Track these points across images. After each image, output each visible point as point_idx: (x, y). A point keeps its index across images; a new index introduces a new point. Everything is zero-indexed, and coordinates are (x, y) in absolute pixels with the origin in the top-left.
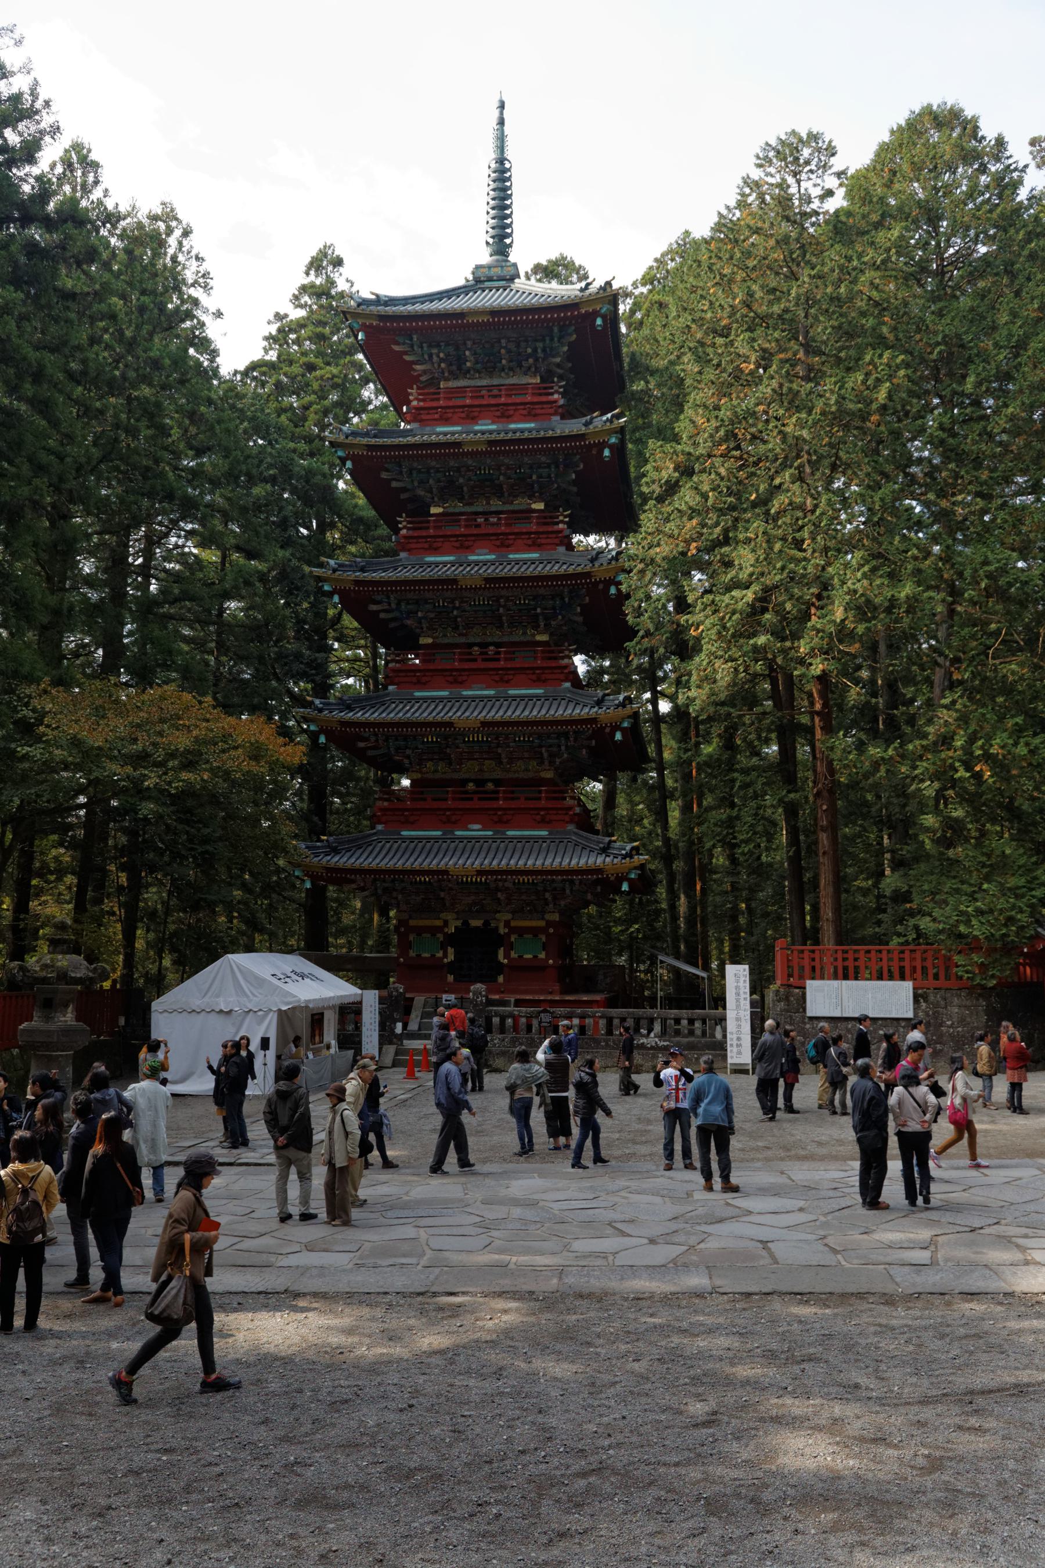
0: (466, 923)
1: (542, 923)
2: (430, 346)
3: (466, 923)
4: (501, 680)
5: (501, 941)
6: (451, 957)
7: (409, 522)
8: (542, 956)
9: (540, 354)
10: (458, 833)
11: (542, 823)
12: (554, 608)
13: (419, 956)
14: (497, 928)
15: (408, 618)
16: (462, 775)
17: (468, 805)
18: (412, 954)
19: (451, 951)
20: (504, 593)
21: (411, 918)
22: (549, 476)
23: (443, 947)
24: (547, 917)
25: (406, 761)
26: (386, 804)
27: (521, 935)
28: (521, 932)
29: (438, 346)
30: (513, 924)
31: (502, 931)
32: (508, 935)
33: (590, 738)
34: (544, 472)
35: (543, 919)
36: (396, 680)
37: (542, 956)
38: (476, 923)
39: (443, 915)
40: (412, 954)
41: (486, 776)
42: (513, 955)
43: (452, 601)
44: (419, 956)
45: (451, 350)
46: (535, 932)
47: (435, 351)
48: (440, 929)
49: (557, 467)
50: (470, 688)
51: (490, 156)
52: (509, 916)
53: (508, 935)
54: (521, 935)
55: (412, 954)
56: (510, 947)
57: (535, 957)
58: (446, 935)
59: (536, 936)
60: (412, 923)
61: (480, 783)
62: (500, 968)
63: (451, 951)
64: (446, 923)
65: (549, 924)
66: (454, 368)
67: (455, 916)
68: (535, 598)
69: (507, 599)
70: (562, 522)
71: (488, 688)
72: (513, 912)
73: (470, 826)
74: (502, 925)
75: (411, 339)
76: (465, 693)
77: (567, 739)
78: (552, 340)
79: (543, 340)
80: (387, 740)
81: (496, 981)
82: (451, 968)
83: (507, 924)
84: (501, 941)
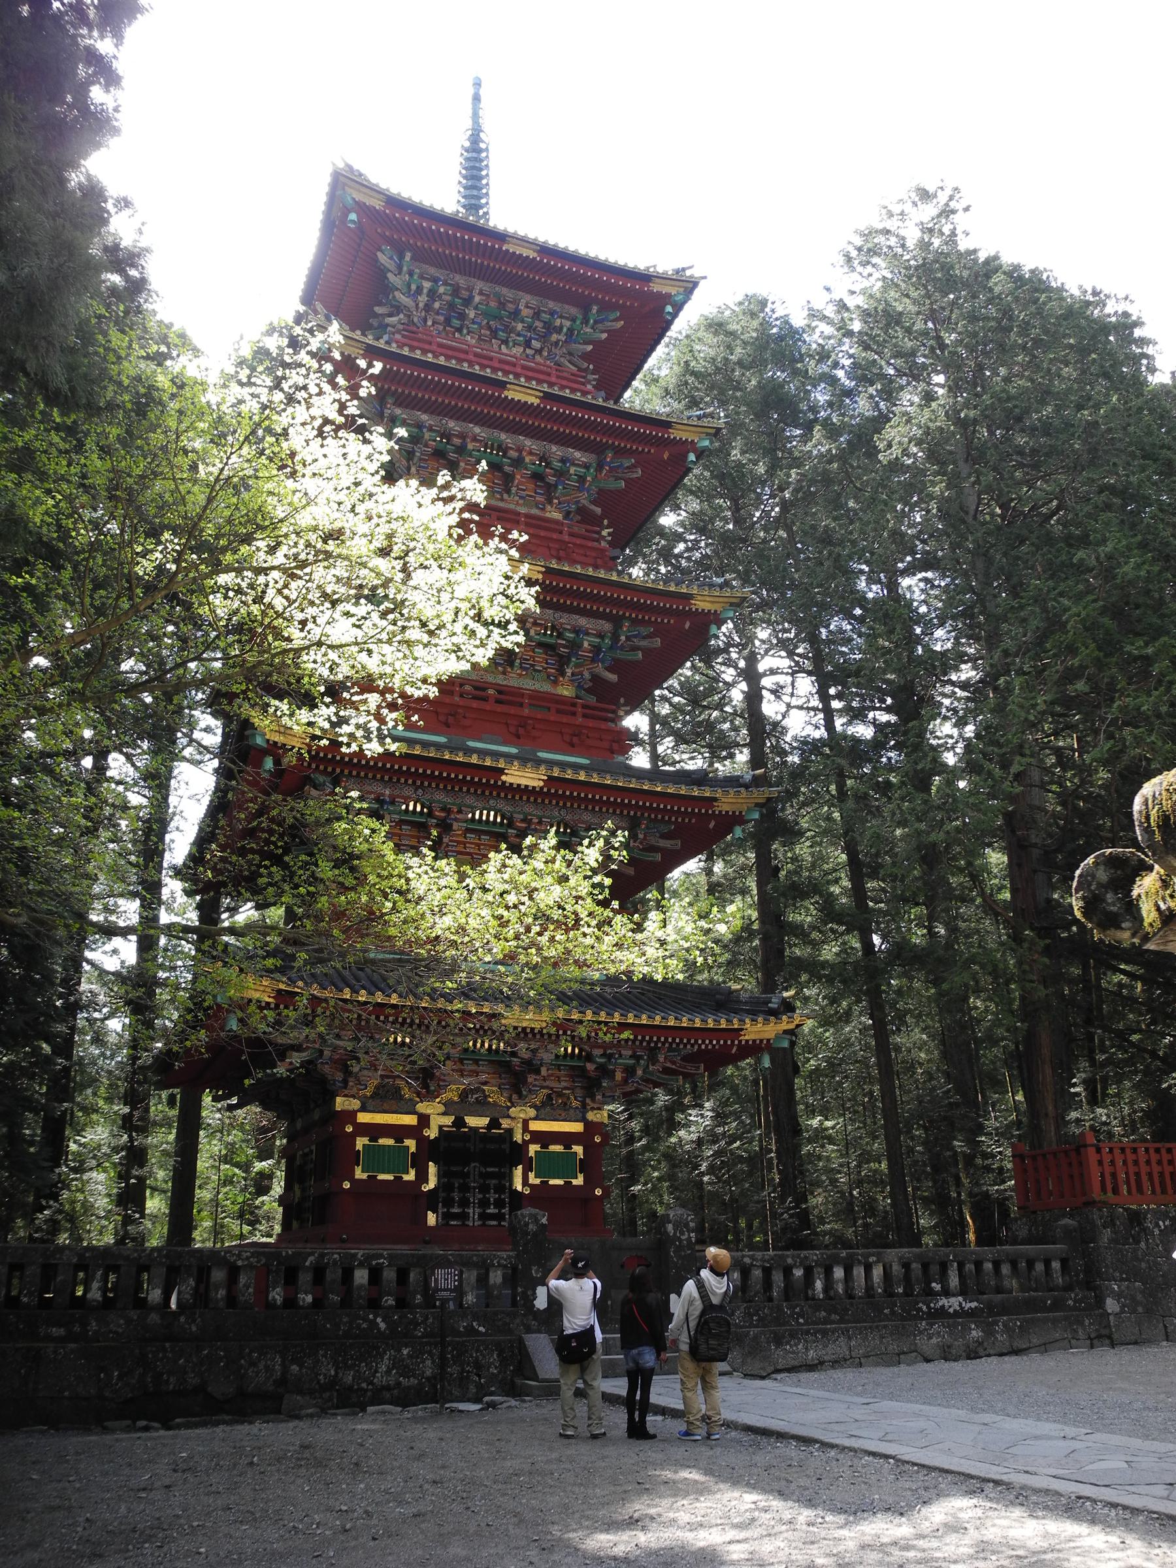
0: (459, 1122)
1: (577, 1127)
2: (422, 277)
3: (459, 1122)
6: (432, 1184)
14: (510, 1132)
18: (360, 1174)
19: (432, 1168)
21: (363, 1109)
22: (582, 479)
29: (435, 280)
30: (535, 1126)
31: (518, 1137)
32: (526, 1143)
37: (579, 1181)
38: (477, 1122)
39: (422, 1107)
40: (360, 1174)
42: (533, 1180)
46: (567, 1139)
47: (427, 285)
48: (414, 1132)
50: (480, 740)
51: (469, 123)
52: (532, 1112)
53: (526, 1143)
57: (568, 1183)
58: (422, 1141)
60: (364, 1118)
63: (432, 1168)
64: (424, 1120)
66: (441, 318)
67: (442, 1108)
68: (577, 631)
71: (505, 743)
75: (401, 257)
76: (471, 744)
78: (585, 321)
79: (573, 320)
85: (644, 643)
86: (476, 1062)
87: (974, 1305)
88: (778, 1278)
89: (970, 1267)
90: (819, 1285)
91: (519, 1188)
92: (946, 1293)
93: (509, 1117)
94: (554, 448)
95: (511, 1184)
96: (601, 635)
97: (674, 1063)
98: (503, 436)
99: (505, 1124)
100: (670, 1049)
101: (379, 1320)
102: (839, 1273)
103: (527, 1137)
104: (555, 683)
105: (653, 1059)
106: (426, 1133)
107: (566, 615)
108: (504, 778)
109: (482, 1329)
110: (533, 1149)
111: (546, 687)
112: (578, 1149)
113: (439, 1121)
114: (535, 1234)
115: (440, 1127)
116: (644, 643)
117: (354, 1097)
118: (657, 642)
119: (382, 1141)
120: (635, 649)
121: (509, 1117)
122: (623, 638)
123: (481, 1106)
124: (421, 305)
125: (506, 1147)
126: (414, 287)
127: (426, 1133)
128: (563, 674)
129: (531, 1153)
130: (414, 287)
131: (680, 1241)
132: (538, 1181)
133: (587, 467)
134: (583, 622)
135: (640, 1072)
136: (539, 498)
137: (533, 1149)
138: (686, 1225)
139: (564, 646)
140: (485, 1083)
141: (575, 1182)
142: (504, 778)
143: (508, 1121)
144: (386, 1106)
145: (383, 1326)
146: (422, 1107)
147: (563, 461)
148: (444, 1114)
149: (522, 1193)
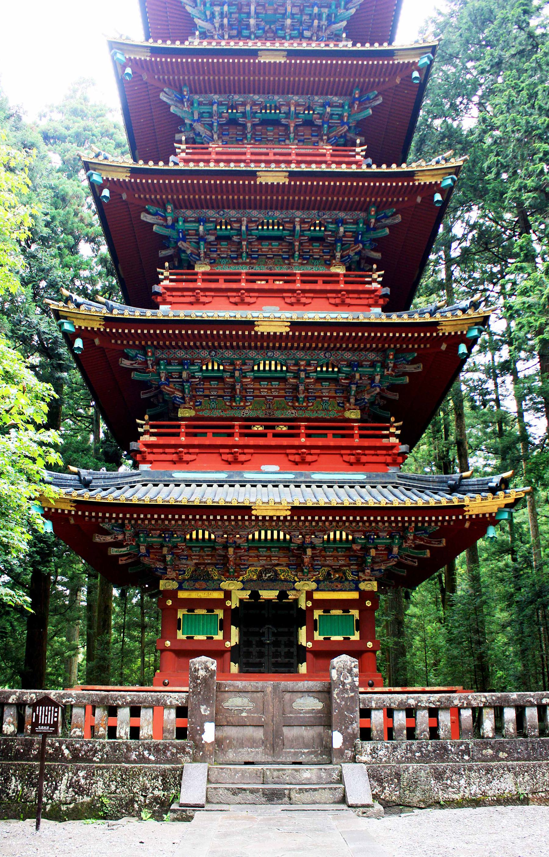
0: (255, 595)
1: (355, 595)
3: (255, 595)
4: (298, 302)
5: (302, 617)
7: (187, 148)
8: (356, 637)
9: (324, 22)
11: (356, 464)
12: (355, 234)
14: (296, 601)
15: (184, 240)
16: (248, 413)
17: (261, 441)
20: (298, 213)
21: (180, 588)
23: (223, 626)
25: (178, 394)
26: (154, 439)
28: (327, 605)
30: (317, 596)
31: (303, 604)
32: (310, 610)
33: (413, 362)
34: (338, 110)
35: (357, 589)
36: (169, 299)
37: (356, 637)
38: (269, 595)
39: (225, 585)
41: (279, 414)
42: (318, 637)
43: (239, 221)
45: (234, 9)
46: (345, 605)
47: (217, 9)
48: (219, 603)
49: (351, 106)
52: (314, 586)
53: (310, 610)
55: (181, 635)
56: (313, 626)
58: (227, 610)
59: (346, 611)
60: (182, 595)
61: (270, 422)
62: (301, 654)
63: (234, 631)
64: (228, 595)
65: (365, 595)
66: (235, 32)
67: (240, 585)
69: (302, 222)
70: (358, 154)
72: (317, 581)
73: (264, 468)
77: (384, 366)
80: (157, 362)
81: (297, 672)
82: (236, 654)
83: (309, 595)
84: (302, 617)
85: (388, 221)
86: (269, 549)
91: (304, 644)
93: (294, 589)
94: (316, 98)
95: (297, 641)
96: (356, 222)
97: (422, 539)
98: (276, 97)
99: (292, 595)
100: (417, 529)
101: (64, 747)
103: (310, 604)
104: (329, 265)
105: (404, 538)
106: (228, 603)
107: (328, 213)
108: (256, 329)
109: (152, 758)
110: (317, 614)
111: (322, 270)
112: (355, 613)
113: (239, 595)
114: (205, 679)
115: (241, 601)
116: (388, 221)
117: (173, 579)
118: (399, 219)
119: (198, 612)
120: (384, 227)
121: (294, 589)
122: (373, 221)
123: (273, 581)
124: (217, 25)
125: (294, 612)
126: (208, 13)
127: (228, 603)
128: (334, 257)
129: (316, 617)
130: (208, 13)
131: (344, 684)
132: (321, 638)
133: (342, 106)
134: (342, 215)
135: (395, 550)
136: (314, 139)
137: (317, 614)
138: (350, 671)
139: (331, 236)
140: (278, 565)
141: (352, 638)
142: (256, 329)
143: (294, 592)
144: (197, 585)
145: (66, 752)
146: (225, 585)
147: (324, 106)
148: (243, 589)
149: (305, 648)
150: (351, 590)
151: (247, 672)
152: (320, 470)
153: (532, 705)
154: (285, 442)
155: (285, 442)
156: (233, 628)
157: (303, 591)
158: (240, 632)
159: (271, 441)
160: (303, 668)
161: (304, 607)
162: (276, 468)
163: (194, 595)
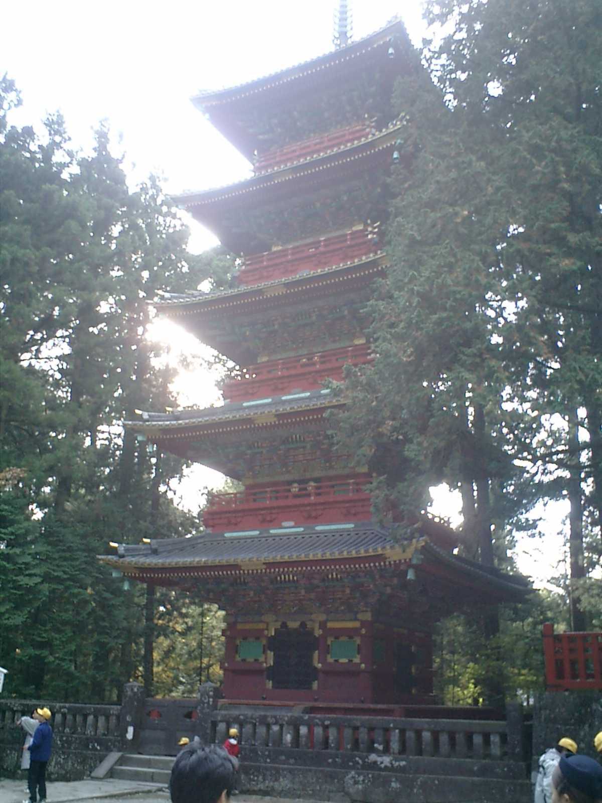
0: (284, 625)
1: (357, 624)
3: (284, 625)
8: (357, 660)
10: (272, 531)
13: (244, 660)
14: (313, 629)
24: (360, 616)
27: (337, 638)
28: (337, 633)
30: (330, 625)
31: (318, 632)
32: (324, 637)
35: (356, 619)
37: (357, 660)
38: (293, 625)
41: (308, 476)
42: (330, 660)
44: (244, 660)
46: (350, 633)
50: (290, 394)
53: (324, 637)
54: (337, 638)
56: (327, 650)
57: (351, 661)
59: (351, 637)
63: (271, 654)
65: (364, 624)
71: (304, 391)
73: (285, 524)
74: (317, 626)
81: (310, 688)
82: (272, 673)
83: (323, 625)
87: (403, 763)
88: (261, 730)
89: (410, 735)
90: (288, 738)
91: (316, 665)
92: (387, 751)
93: (311, 620)
102: (303, 730)
112: (358, 641)
121: (311, 620)
148: (276, 621)
150: (351, 620)
151: (277, 688)
152: (321, 524)
153: (317, 725)
154: (298, 501)
155: (298, 501)
156: (269, 652)
157: (316, 623)
158: (274, 655)
159: (290, 502)
160: (315, 685)
161: (317, 635)
162: (292, 523)
163: (248, 627)
